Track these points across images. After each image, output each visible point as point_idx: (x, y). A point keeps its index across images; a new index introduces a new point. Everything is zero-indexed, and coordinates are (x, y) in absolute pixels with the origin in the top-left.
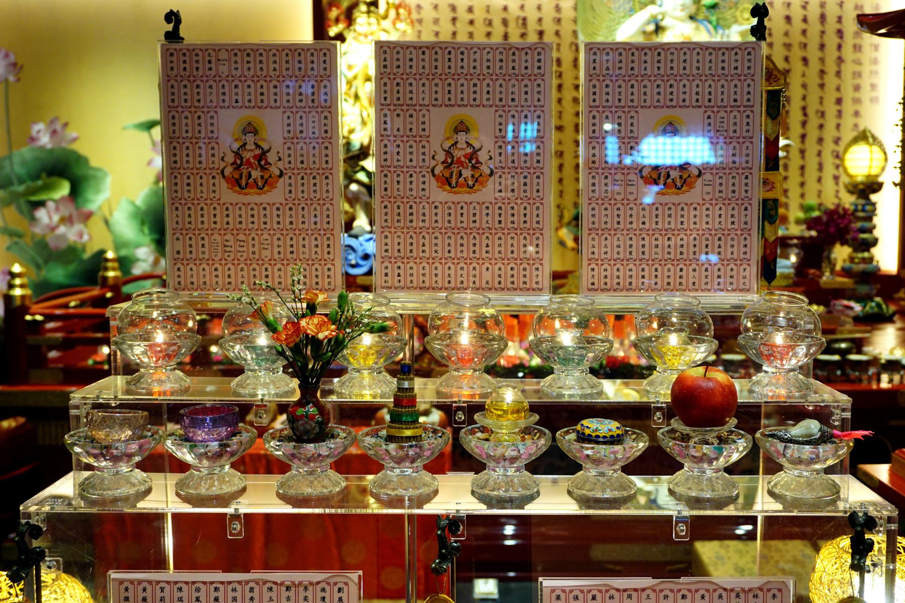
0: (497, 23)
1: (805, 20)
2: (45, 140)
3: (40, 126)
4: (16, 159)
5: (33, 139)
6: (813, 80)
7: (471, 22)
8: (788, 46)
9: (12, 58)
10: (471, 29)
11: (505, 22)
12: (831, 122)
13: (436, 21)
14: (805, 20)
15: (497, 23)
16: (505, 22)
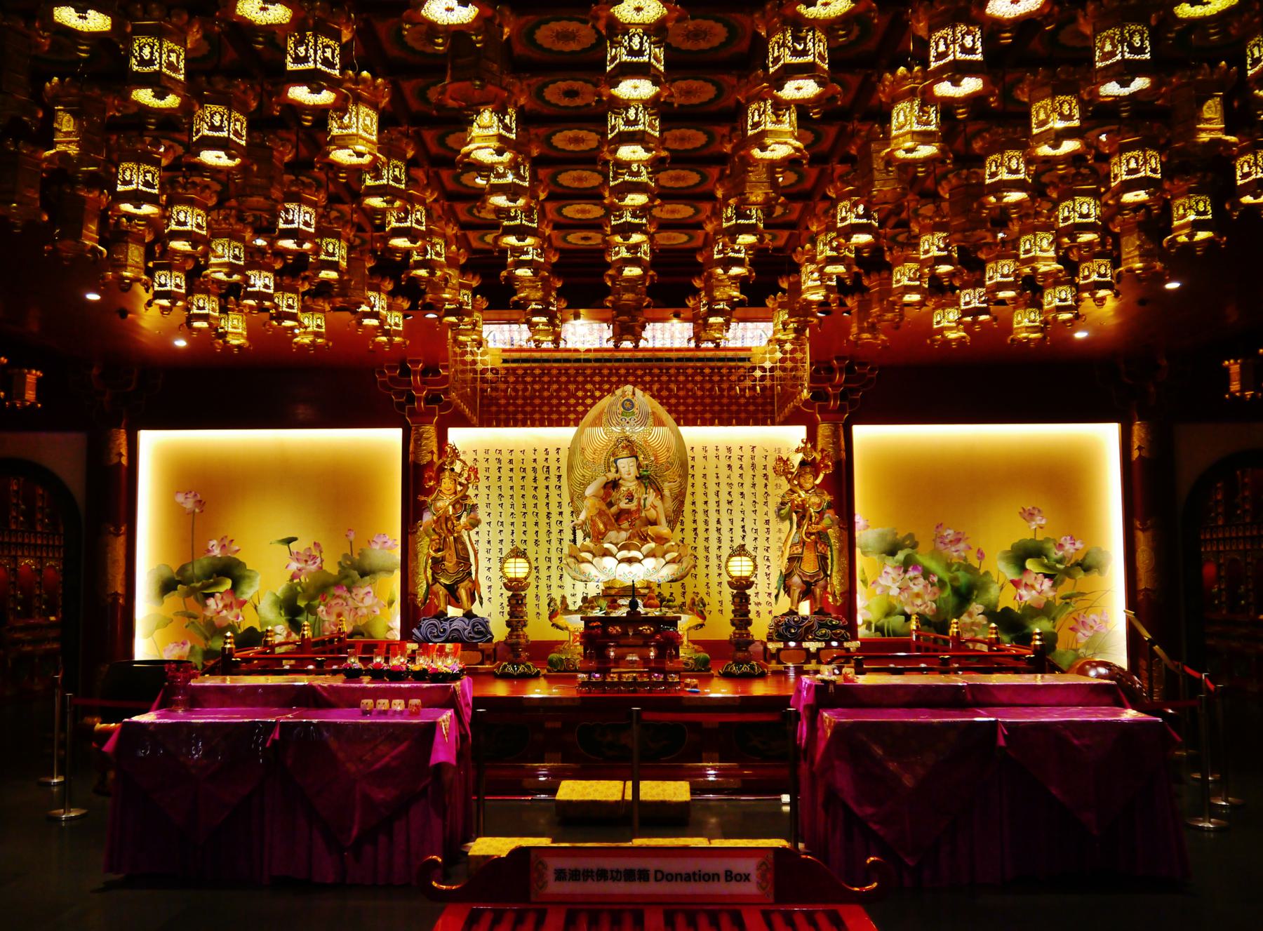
0: (529, 470)
1: (741, 467)
2: (217, 552)
3: (214, 542)
4: (197, 566)
5: (209, 551)
6: (748, 507)
7: (511, 470)
8: (730, 485)
9: (199, 497)
10: (511, 474)
11: (534, 469)
12: (762, 535)
13: (487, 469)
14: (741, 467)
15: (529, 470)
16: (534, 469)
